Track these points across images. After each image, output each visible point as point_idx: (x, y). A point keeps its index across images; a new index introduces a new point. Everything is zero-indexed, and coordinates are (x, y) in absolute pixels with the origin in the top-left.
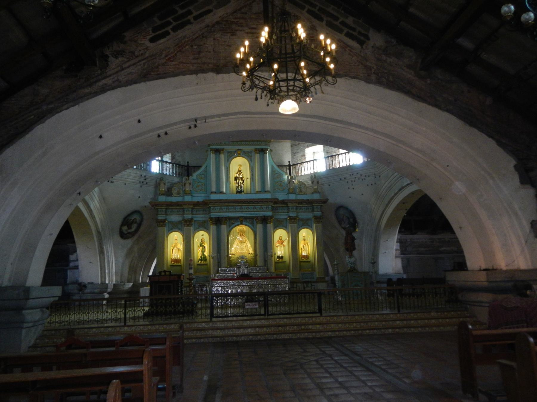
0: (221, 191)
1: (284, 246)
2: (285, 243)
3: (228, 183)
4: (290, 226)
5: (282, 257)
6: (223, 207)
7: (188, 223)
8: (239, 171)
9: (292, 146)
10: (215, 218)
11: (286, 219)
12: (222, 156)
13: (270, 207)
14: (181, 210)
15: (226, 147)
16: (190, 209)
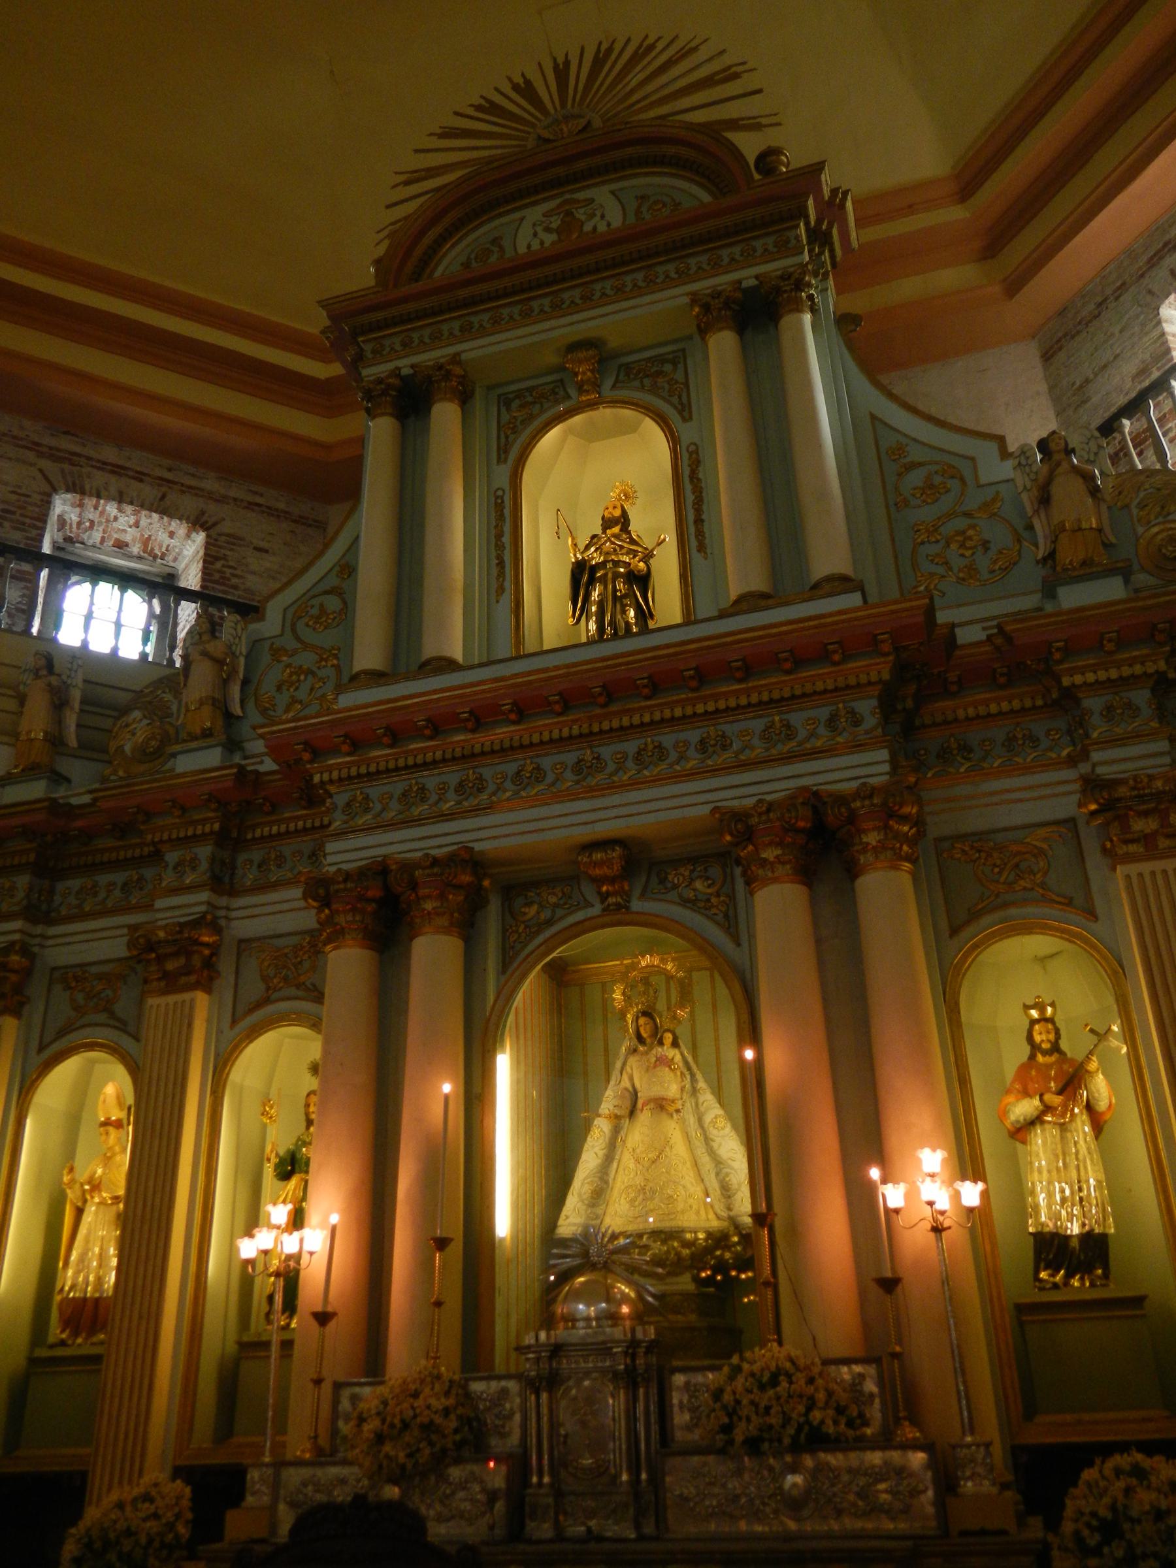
0: (429, 650)
1: (1098, 1123)
2: (1100, 1087)
3: (507, 598)
4: (1117, 886)
5: (1092, 1252)
6: (431, 780)
7: (180, 960)
8: (607, 523)
9: (1047, 357)
10: (361, 874)
11: (1071, 822)
12: (445, 415)
13: (867, 707)
14: (148, 873)
15: (473, 350)
16: (204, 852)
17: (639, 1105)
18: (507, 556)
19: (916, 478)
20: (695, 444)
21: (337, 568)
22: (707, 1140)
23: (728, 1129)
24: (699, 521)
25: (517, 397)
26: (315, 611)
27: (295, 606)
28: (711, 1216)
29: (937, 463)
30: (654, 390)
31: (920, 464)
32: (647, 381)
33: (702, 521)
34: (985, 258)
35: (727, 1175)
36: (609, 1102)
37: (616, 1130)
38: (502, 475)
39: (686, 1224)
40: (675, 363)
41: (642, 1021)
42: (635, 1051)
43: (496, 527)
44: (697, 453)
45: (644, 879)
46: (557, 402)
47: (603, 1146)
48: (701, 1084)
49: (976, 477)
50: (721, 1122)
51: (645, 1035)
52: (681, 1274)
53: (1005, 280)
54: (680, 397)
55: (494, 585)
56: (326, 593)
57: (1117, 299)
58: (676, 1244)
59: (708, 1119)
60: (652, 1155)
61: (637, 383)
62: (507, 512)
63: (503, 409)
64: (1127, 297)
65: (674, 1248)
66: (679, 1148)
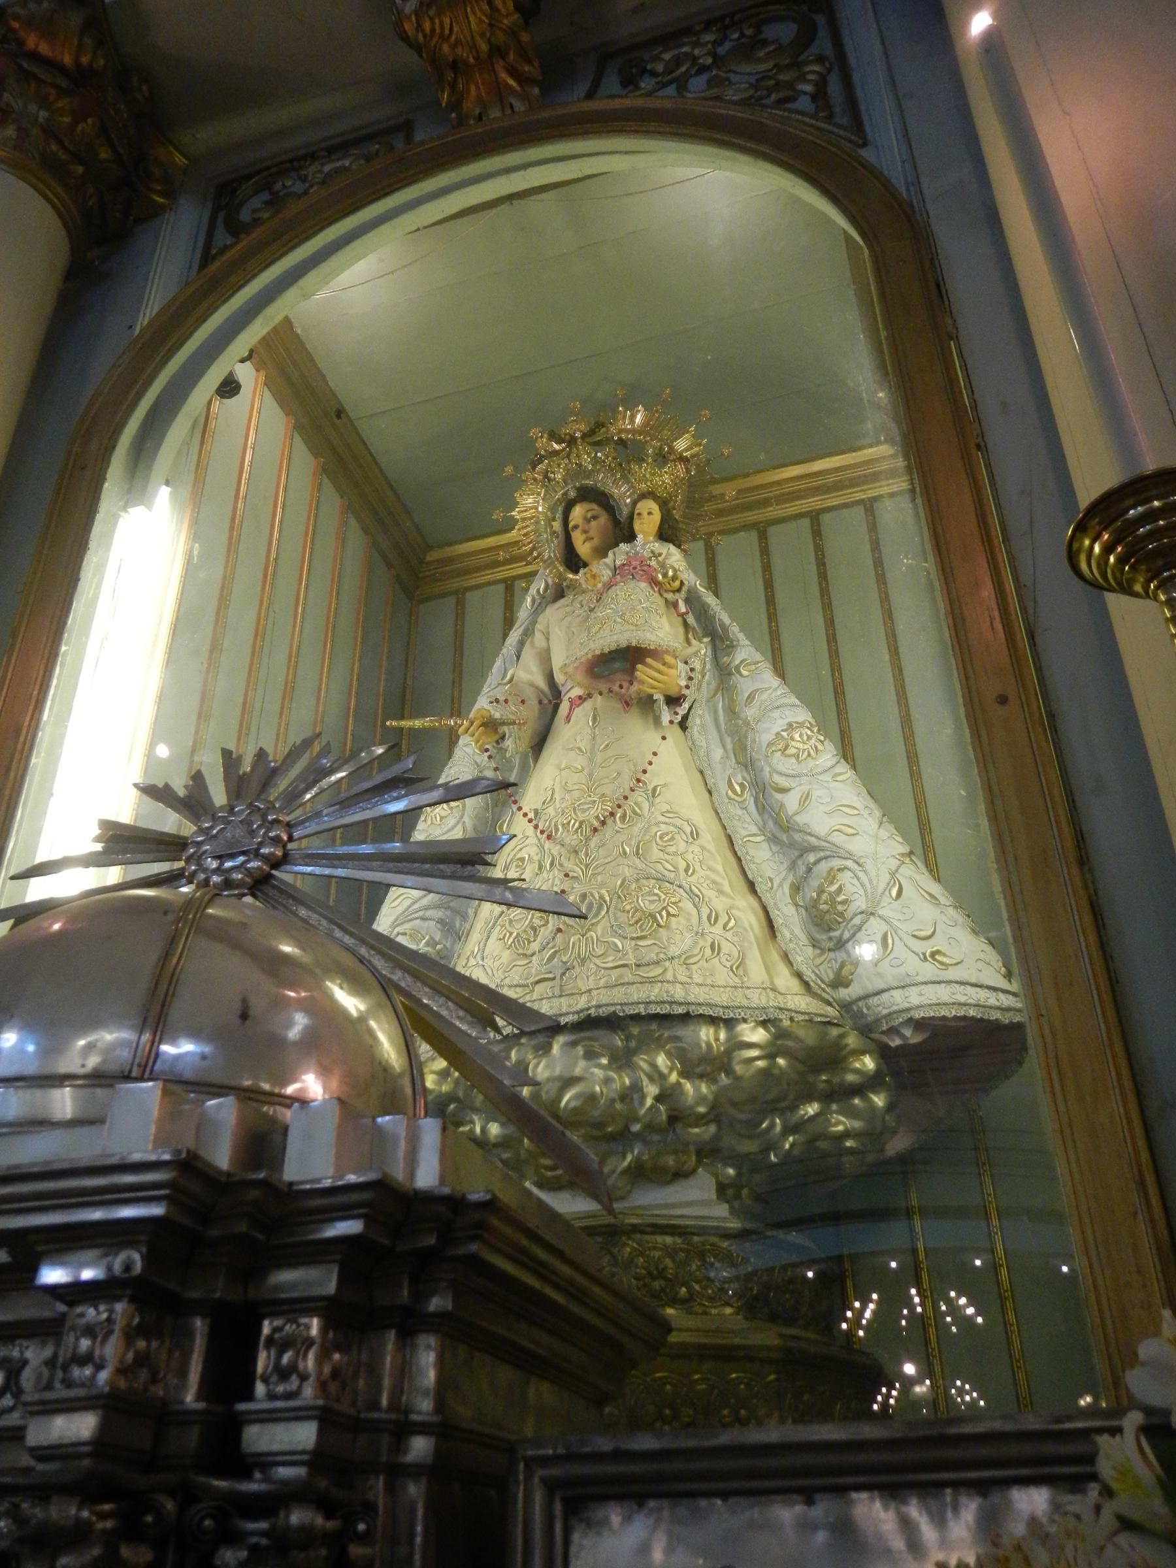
22: (763, 794)
28: (785, 980)
39: (698, 995)
51: (583, 548)
52: (679, 1175)
58: (661, 1060)
65: (658, 1076)
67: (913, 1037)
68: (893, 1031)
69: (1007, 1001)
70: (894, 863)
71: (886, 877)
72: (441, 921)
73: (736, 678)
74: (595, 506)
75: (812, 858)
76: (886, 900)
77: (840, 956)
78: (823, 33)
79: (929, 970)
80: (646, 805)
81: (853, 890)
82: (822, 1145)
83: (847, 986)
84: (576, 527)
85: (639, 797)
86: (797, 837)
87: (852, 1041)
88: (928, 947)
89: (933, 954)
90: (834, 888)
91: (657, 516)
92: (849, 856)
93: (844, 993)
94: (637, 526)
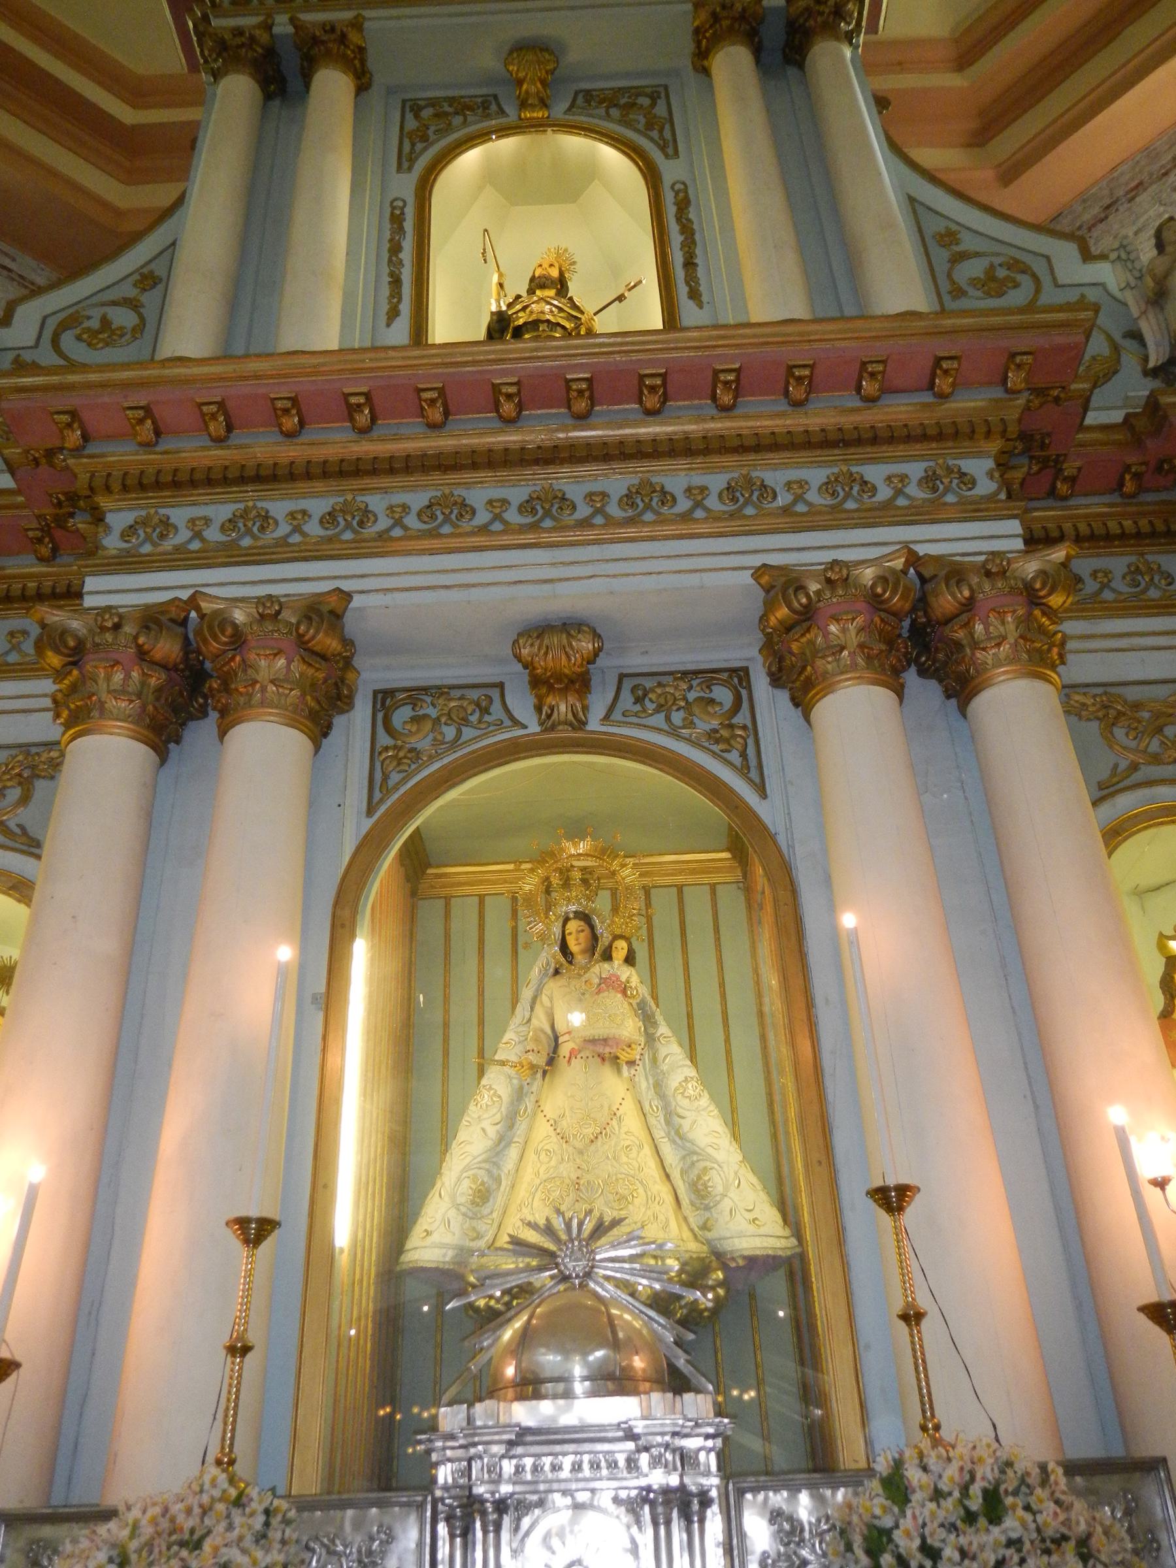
17: (564, 1050)
18: (407, 275)
19: (972, 269)
20: (684, 183)
21: (137, 277)
22: (670, 1115)
23: (705, 1101)
24: (690, 264)
25: (433, 105)
26: (95, 324)
27: (61, 316)
28: (687, 1234)
29: (998, 254)
30: (625, 122)
31: (977, 255)
32: (614, 112)
33: (696, 265)
34: (969, 145)
35: (705, 1170)
36: (511, 1044)
37: (519, 1095)
38: (404, 186)
40: (654, 98)
41: (573, 926)
42: (557, 972)
43: (391, 240)
44: (686, 192)
45: (610, 696)
46: (488, 116)
47: (498, 1117)
48: (663, 1029)
49: (1054, 279)
50: (692, 1088)
51: (574, 947)
53: (999, 165)
54: (661, 131)
55: (385, 307)
56: (114, 303)
57: (1131, 200)
59: (674, 1081)
60: (589, 1131)
61: (601, 111)
62: (409, 225)
63: (409, 116)
64: (1143, 198)
66: (632, 1122)
67: (741, 1263)
68: (733, 1259)
69: (783, 1243)
70: (736, 1167)
71: (732, 1175)
72: (488, 1171)
73: (657, 1044)
74: (582, 923)
75: (695, 1158)
76: (733, 1188)
77: (707, 1215)
78: (745, 705)
79: (751, 1229)
80: (616, 1128)
81: (716, 1181)
82: (695, 1314)
83: (709, 1230)
84: (570, 934)
85: (614, 1123)
86: (688, 1144)
87: (714, 1264)
88: (750, 1216)
89: (754, 1220)
90: (706, 1178)
91: (625, 951)
92: (716, 1162)
93: (709, 1235)
94: (614, 955)
